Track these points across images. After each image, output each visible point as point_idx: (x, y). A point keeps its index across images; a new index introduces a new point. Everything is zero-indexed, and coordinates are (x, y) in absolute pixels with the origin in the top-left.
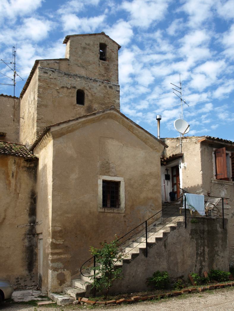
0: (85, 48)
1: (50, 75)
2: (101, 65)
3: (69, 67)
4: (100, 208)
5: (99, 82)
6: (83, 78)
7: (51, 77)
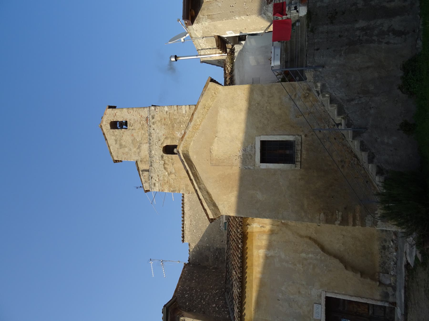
0: (121, 145)
1: (156, 180)
2: (132, 128)
3: (144, 161)
4: (296, 167)
5: (151, 131)
6: (150, 148)
7: (157, 180)
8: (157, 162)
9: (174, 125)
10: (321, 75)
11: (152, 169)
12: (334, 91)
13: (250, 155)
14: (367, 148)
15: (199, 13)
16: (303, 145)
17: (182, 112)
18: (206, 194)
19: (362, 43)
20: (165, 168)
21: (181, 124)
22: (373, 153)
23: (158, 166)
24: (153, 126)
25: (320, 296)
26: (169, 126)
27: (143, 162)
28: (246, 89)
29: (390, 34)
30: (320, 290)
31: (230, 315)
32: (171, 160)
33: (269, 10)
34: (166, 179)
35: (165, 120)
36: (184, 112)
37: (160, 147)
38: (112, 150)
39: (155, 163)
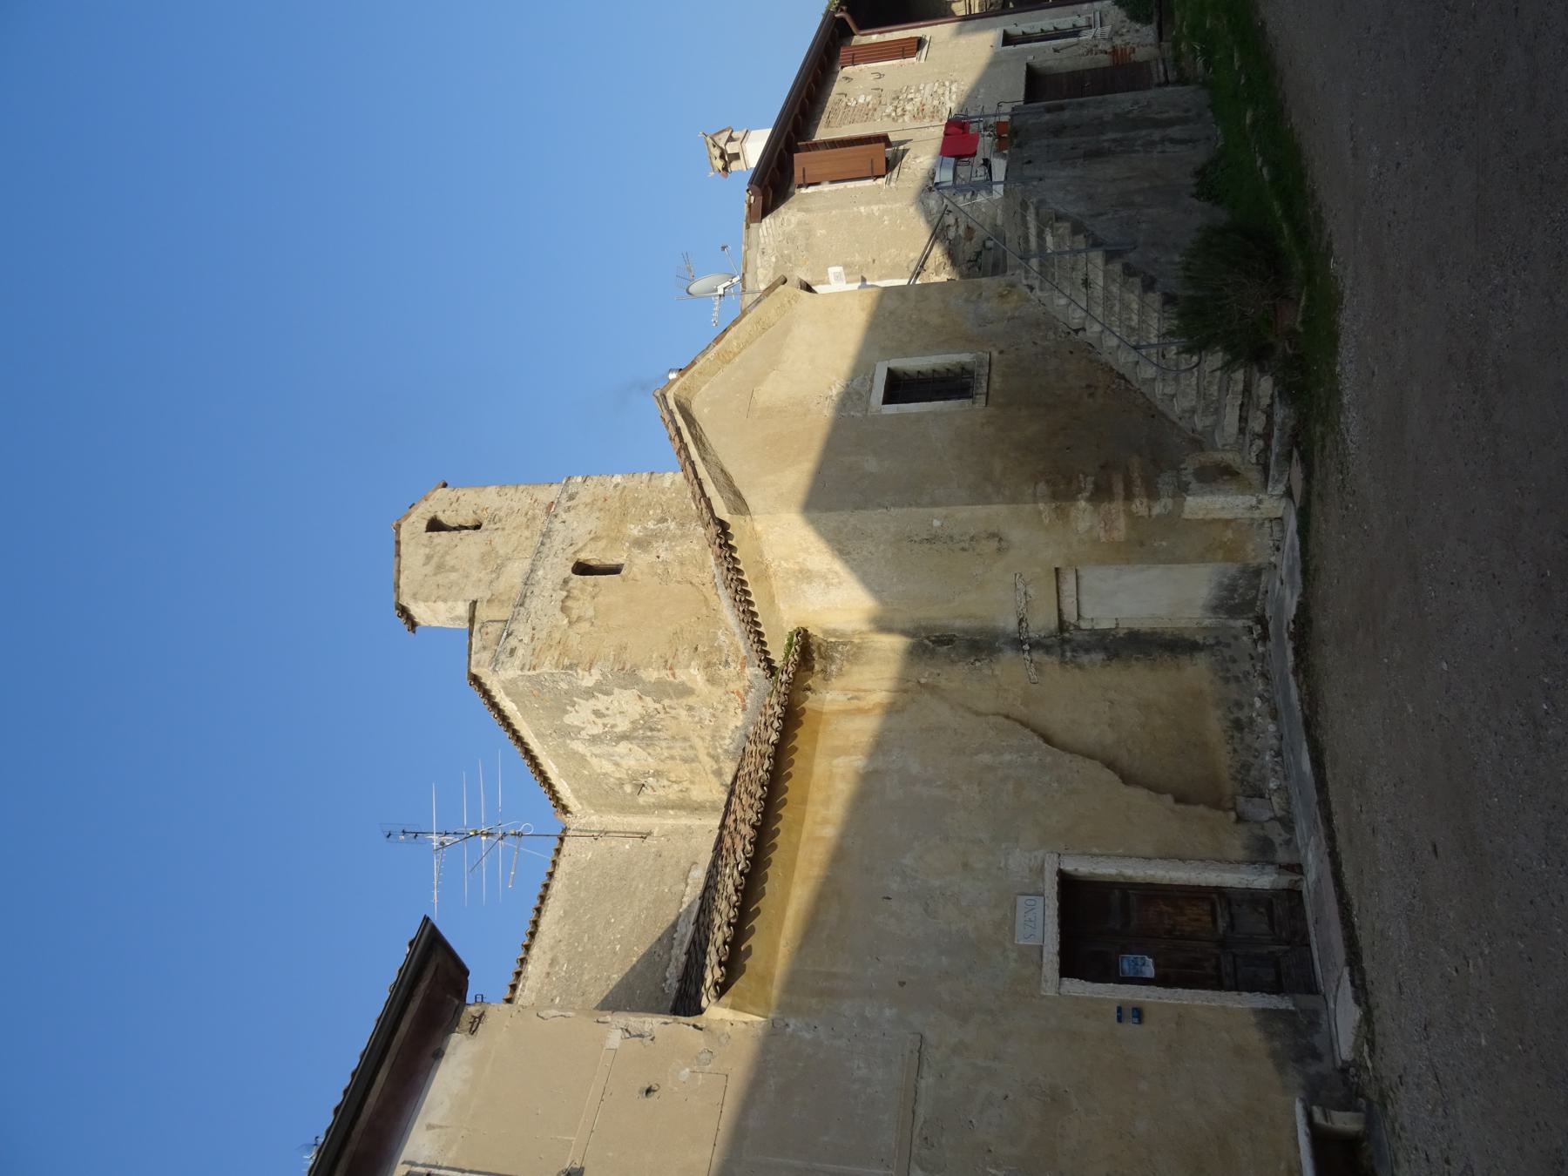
5: (552, 526)
7: (526, 640)
16: (993, 367)
25: (1042, 870)
30: (1040, 854)
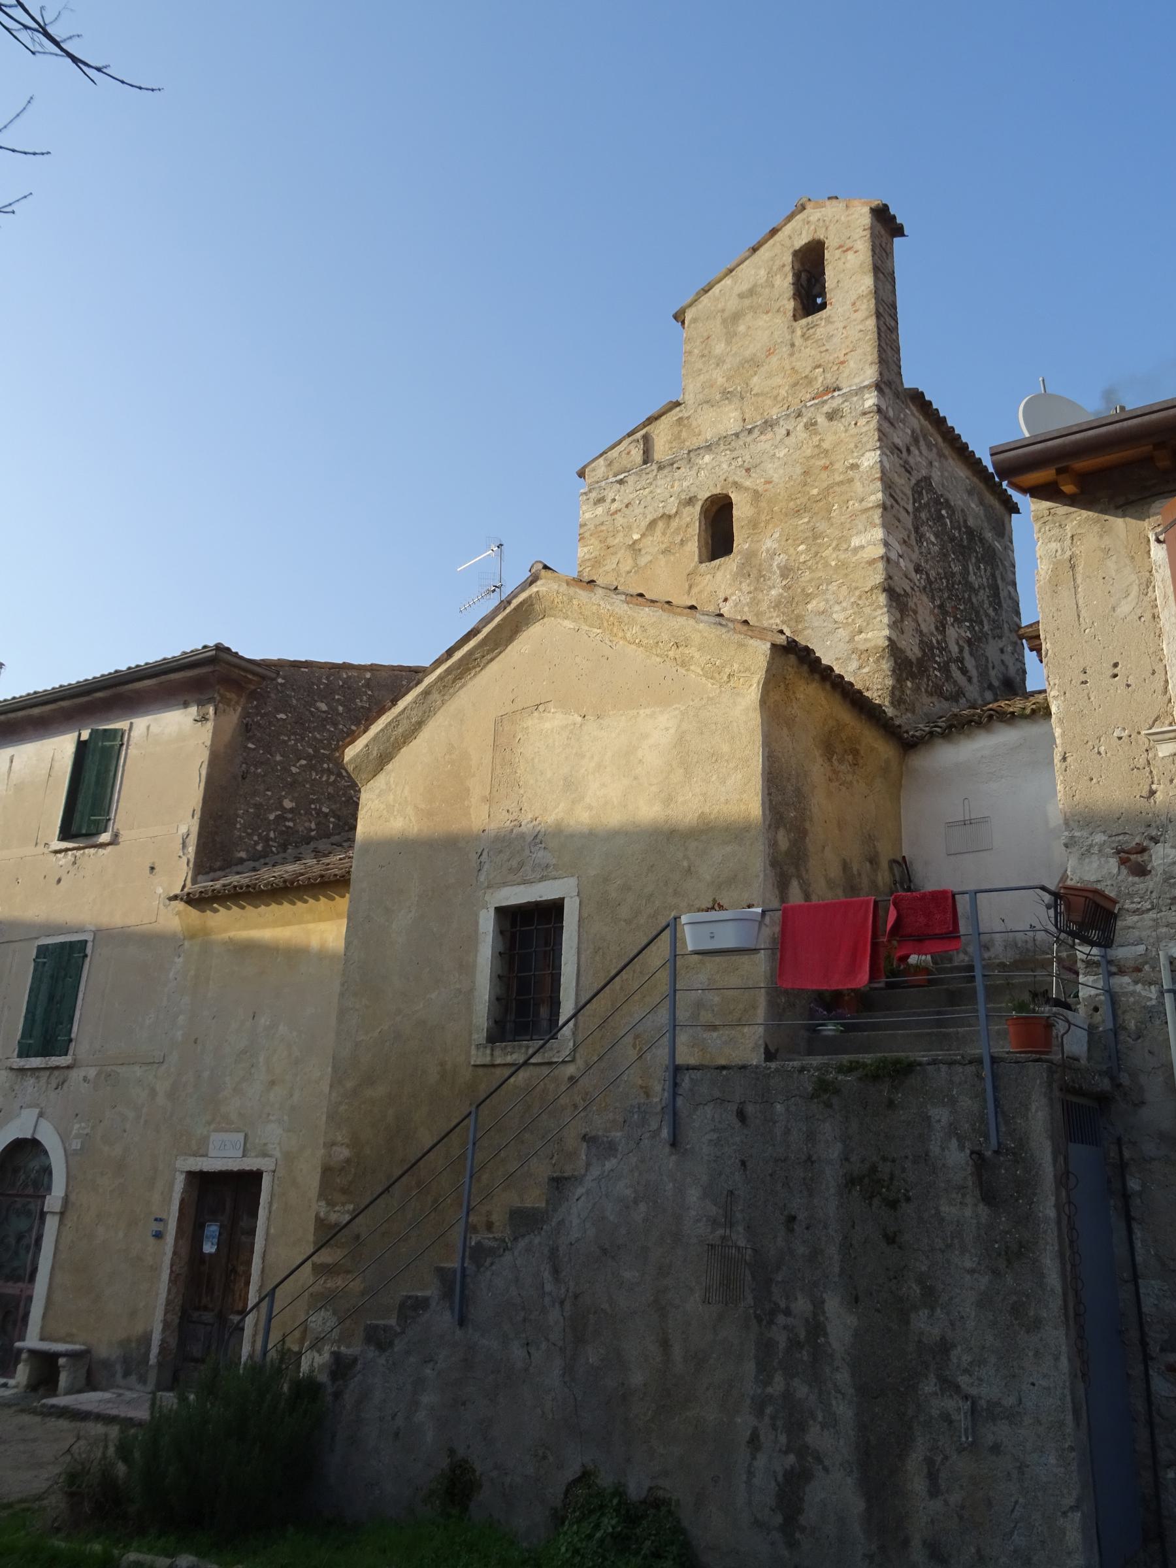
0: (736, 317)
1: (614, 500)
2: (798, 341)
3: (681, 431)
4: (478, 1046)
5: (782, 423)
7: (614, 506)
8: (672, 487)
9: (806, 514)
10: (648, 1134)
11: (650, 476)
12: (588, 1192)
13: (521, 864)
14: (409, 1322)
15: (1085, 514)
17: (855, 532)
18: (413, 720)
19: (759, 1319)
20: (652, 524)
21: (810, 541)
22: (391, 1344)
23: (659, 494)
24: (800, 427)
25: (265, 1155)
26: (799, 495)
27: (676, 429)
28: (743, 807)
29: (791, 1459)
30: (278, 1154)
31: (249, 860)
32: (680, 538)
33: (1087, 860)
34: (617, 541)
35: (823, 471)
36: (855, 542)
37: (725, 480)
38: (718, 291)
39: (668, 480)
